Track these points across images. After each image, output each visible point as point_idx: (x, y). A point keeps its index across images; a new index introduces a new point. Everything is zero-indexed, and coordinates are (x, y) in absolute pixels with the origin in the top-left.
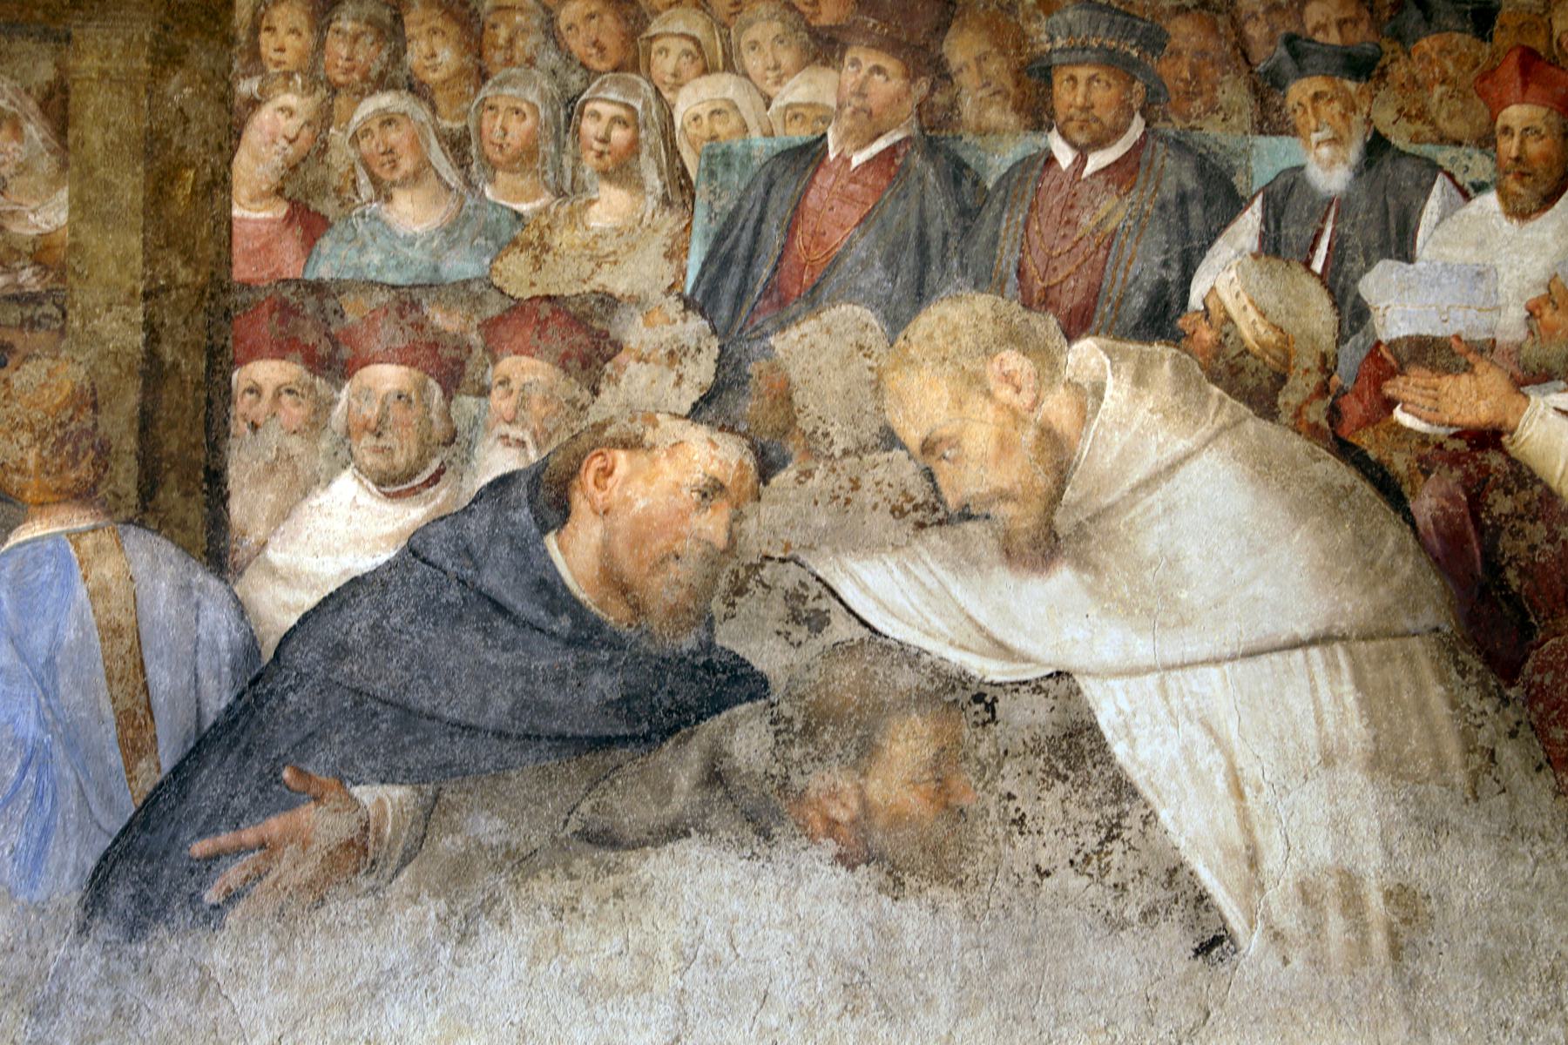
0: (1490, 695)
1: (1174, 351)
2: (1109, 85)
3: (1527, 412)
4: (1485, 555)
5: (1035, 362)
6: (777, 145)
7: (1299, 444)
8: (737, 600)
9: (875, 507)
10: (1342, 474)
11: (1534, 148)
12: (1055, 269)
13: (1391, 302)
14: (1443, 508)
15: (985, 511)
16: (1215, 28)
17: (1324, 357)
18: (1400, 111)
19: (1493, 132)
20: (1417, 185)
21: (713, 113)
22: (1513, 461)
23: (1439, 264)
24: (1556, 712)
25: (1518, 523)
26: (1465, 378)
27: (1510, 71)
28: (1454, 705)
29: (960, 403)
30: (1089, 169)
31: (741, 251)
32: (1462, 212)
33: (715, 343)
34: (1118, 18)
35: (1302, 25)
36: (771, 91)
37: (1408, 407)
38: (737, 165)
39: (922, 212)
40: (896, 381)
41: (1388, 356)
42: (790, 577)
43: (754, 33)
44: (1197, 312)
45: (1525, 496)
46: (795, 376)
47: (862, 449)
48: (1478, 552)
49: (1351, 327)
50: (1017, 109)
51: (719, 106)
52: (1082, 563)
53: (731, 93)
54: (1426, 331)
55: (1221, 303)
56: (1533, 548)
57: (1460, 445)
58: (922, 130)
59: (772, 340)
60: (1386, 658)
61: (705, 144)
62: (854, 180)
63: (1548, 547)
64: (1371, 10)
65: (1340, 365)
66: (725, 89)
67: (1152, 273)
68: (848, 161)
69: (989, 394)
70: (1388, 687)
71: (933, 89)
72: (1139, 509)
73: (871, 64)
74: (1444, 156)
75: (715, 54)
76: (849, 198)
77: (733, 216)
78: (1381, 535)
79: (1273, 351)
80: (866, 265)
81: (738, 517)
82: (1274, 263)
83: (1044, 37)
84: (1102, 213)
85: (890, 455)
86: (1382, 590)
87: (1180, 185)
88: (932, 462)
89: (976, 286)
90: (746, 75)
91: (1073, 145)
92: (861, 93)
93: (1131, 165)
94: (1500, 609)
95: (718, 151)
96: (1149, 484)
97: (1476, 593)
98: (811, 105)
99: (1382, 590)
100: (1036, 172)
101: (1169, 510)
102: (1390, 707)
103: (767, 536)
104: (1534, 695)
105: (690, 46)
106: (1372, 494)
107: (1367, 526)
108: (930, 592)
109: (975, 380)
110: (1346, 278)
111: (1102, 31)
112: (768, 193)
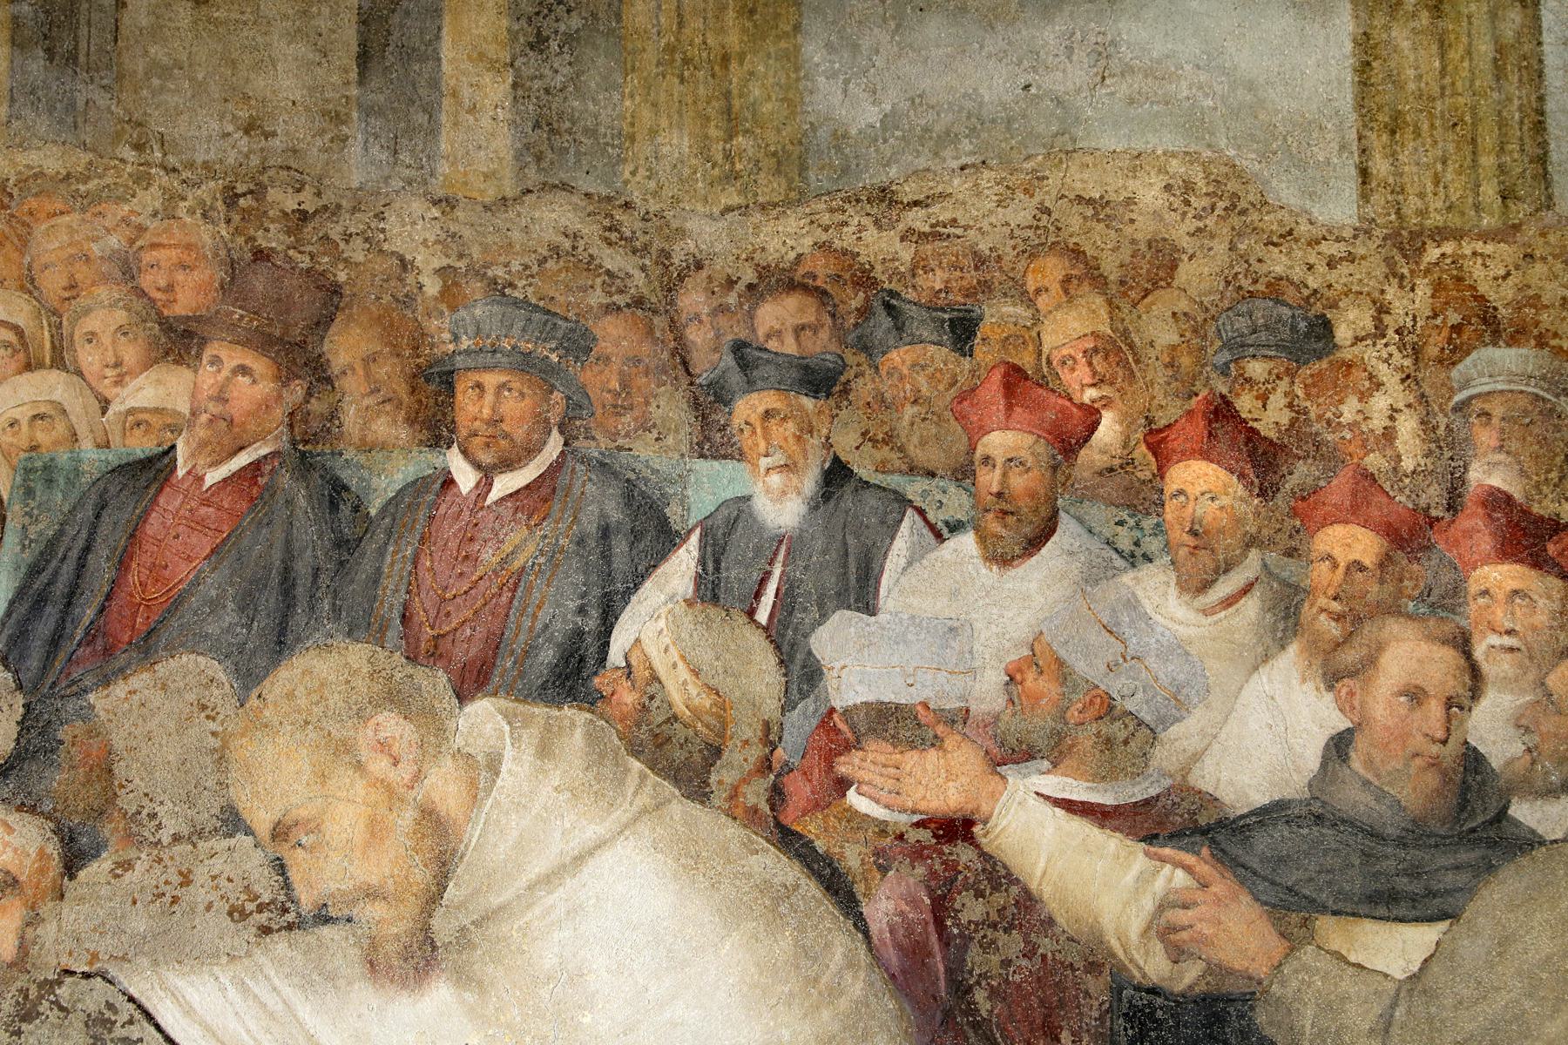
1: (588, 716)
2: (522, 395)
3: (1004, 798)
4: (949, 971)
5: (417, 727)
6: (112, 458)
7: (733, 832)
8: (24, 1027)
9: (209, 908)
10: (785, 870)
11: (1018, 482)
12: (448, 614)
13: (848, 661)
14: (902, 913)
15: (346, 912)
16: (650, 331)
17: (767, 726)
18: (864, 434)
19: (972, 463)
20: (883, 523)
21: (35, 417)
22: (985, 856)
23: (906, 617)
26: (932, 754)
27: (993, 390)
29: (323, 777)
30: (494, 495)
31: (60, 587)
32: (932, 556)
33: (20, 700)
34: (537, 316)
35: (754, 331)
36: (109, 392)
37: (865, 788)
38: (62, 481)
39: (288, 542)
40: (244, 749)
41: (842, 726)
42: (94, 996)
43: (92, 323)
44: (618, 668)
45: (999, 899)
46: (118, 742)
47: (199, 833)
48: (941, 968)
49: (800, 690)
50: (411, 421)
51: (43, 410)
52: (464, 978)
53: (56, 396)
54: (888, 697)
55: (647, 658)
56: (1006, 963)
57: (925, 835)
58: (294, 443)
59: (92, 697)
61: (23, 455)
62: (206, 502)
63: (1024, 962)
64: (833, 316)
65: (786, 736)
66: (52, 389)
67: (565, 621)
68: (201, 479)
69: (359, 766)
71: (309, 394)
72: (537, 910)
73: (235, 363)
74: (914, 488)
75: (42, 346)
76: (200, 525)
77: (52, 544)
78: (828, 946)
79: (707, 718)
80: (215, 605)
81: (33, 920)
82: (712, 611)
83: (447, 336)
84: (507, 548)
85: (232, 841)
86: (826, 1014)
87: (603, 515)
88: (284, 851)
89: (349, 634)
90: (79, 373)
91: (478, 466)
92: (221, 398)
93: (545, 491)
94: (967, 1039)
95: (39, 464)
96: (549, 880)
97: (939, 1017)
98: (157, 411)
99: (826, 1014)
100: (430, 497)
101: (573, 911)
103: (69, 944)
105: (10, 336)
106: (819, 895)
107: (811, 935)
108: (272, 1015)
109: (344, 749)
110: (796, 630)
111: (516, 331)
112: (98, 516)
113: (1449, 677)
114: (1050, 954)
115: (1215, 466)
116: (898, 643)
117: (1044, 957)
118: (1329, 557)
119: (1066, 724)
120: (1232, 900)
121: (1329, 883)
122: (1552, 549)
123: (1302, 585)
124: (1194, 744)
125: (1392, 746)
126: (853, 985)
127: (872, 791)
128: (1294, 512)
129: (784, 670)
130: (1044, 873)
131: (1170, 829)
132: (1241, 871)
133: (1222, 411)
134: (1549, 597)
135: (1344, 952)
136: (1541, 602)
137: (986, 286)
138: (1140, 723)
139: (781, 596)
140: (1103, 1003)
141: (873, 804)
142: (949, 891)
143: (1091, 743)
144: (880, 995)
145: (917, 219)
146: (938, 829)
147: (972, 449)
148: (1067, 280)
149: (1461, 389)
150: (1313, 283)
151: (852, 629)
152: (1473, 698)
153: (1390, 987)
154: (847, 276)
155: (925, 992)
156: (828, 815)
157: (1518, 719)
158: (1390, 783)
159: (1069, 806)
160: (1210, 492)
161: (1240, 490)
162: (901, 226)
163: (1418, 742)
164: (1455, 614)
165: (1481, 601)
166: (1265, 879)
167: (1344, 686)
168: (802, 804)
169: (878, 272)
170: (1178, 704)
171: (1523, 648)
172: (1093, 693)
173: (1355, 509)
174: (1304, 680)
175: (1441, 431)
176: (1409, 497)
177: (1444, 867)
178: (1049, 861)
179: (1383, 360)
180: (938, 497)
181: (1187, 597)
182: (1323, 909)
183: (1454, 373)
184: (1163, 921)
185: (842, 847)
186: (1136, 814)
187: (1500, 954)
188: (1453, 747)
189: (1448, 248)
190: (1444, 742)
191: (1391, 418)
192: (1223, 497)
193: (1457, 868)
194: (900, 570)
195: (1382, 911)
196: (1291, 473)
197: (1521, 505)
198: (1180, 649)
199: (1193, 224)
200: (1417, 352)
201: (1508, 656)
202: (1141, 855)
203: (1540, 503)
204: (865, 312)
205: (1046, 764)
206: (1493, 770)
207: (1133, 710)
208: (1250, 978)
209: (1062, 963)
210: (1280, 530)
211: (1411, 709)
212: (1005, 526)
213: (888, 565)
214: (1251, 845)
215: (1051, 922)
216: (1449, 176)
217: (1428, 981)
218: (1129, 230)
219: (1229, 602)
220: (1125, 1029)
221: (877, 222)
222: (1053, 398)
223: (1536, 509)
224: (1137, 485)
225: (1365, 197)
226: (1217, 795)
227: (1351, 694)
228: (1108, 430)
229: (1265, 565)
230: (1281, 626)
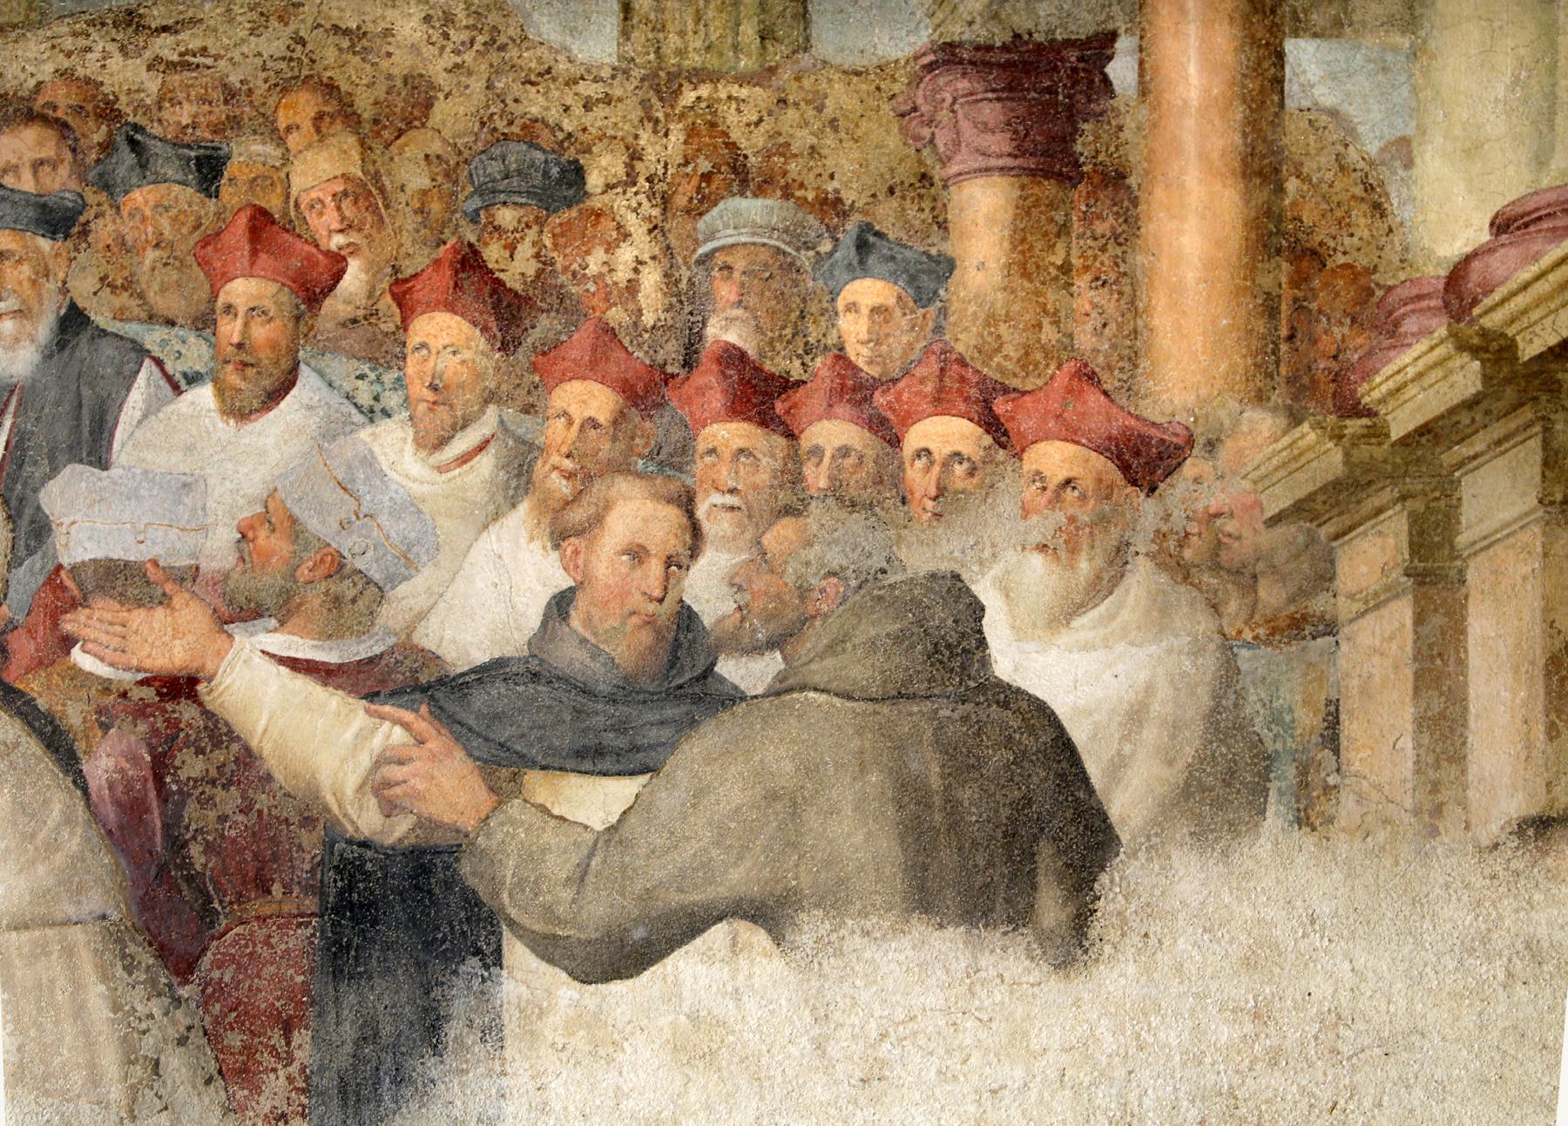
0: (159, 995)
3: (229, 656)
4: (166, 827)
11: (260, 332)
13: (78, 517)
14: (122, 771)
18: (102, 279)
19: (213, 311)
20: (119, 373)
22: (208, 714)
23: (138, 471)
24: (234, 1014)
25: (208, 789)
26: (160, 612)
27: (238, 234)
28: (116, 1008)
32: (170, 408)
37: (90, 646)
41: (69, 583)
45: (219, 756)
48: (158, 824)
49: (27, 546)
56: (223, 818)
57: (149, 693)
60: (40, 951)
63: (240, 818)
64: (74, 150)
70: (40, 985)
74: (153, 337)
86: (41, 869)
99: (41, 869)
102: (40, 1010)
104: (211, 993)
107: (30, 791)
110: (25, 484)
113: (671, 537)
114: (266, 810)
115: (458, 318)
116: (129, 499)
117: (260, 812)
118: (565, 413)
119: (296, 582)
120: (446, 756)
121: (540, 739)
122: (780, 407)
123: (537, 442)
124: (421, 602)
125: (611, 605)
126: (69, 840)
127: (97, 649)
128: (534, 367)
129: (11, 526)
130: (265, 730)
131: (392, 686)
132: (457, 727)
133: (469, 262)
134: (773, 456)
135: (548, 805)
136: (765, 461)
137: (235, 122)
138: (369, 581)
139: (10, 448)
140: (315, 856)
141: (98, 662)
142: (170, 748)
143: (319, 601)
144: (97, 850)
145: (165, 47)
146: (162, 687)
147: (215, 296)
148: (319, 117)
149: (706, 241)
150: (568, 125)
151: (83, 484)
152: (691, 557)
153: (589, 838)
154: (90, 107)
155: (141, 847)
156: (51, 674)
157: (732, 578)
158: (605, 641)
159: (294, 664)
160: (452, 345)
161: (482, 344)
162: (148, 54)
163: (636, 600)
164: (682, 472)
165: (708, 459)
166: (479, 735)
167: (570, 545)
168: (26, 662)
169: (123, 104)
170: (408, 563)
171: (743, 507)
172: (325, 551)
173: (594, 364)
174: (532, 539)
175: (683, 285)
176: (647, 352)
177: (649, 723)
178: (270, 718)
179: (634, 211)
180: (177, 347)
181: (423, 454)
182: (533, 764)
183: (701, 225)
184: (378, 777)
185: (64, 705)
186: (359, 672)
187: (694, 806)
188: (669, 605)
189: (705, 91)
190: (661, 601)
191: (636, 270)
192: (465, 351)
193: (662, 723)
194: (135, 423)
195: (587, 765)
196: (533, 327)
197: (753, 362)
198: (412, 507)
199: (449, 60)
200: (666, 201)
201: (729, 515)
202: (361, 713)
203: (772, 360)
204: (107, 147)
205: (273, 622)
206: (704, 628)
207: (363, 568)
208: (458, 831)
209: (277, 818)
210: (519, 385)
211: (633, 568)
212: (245, 379)
213: (123, 418)
214: (469, 704)
215: (269, 778)
216: (710, 14)
217: (625, 832)
218: (385, 64)
219: (464, 459)
220: (335, 881)
221: (122, 49)
222: (299, 245)
223: (768, 366)
224: (380, 336)
225: (625, 34)
226: (439, 653)
227: (576, 552)
228: (354, 278)
229: (502, 422)
230: (514, 484)
